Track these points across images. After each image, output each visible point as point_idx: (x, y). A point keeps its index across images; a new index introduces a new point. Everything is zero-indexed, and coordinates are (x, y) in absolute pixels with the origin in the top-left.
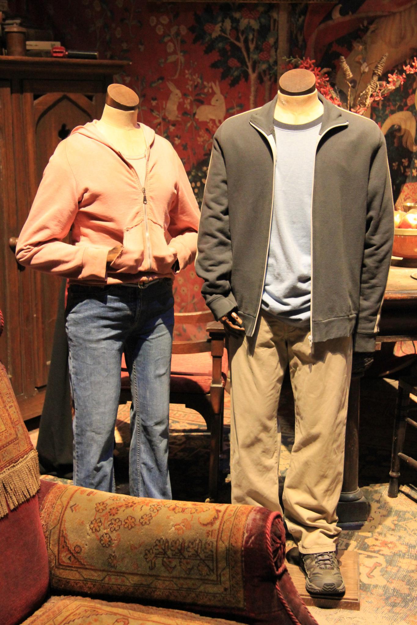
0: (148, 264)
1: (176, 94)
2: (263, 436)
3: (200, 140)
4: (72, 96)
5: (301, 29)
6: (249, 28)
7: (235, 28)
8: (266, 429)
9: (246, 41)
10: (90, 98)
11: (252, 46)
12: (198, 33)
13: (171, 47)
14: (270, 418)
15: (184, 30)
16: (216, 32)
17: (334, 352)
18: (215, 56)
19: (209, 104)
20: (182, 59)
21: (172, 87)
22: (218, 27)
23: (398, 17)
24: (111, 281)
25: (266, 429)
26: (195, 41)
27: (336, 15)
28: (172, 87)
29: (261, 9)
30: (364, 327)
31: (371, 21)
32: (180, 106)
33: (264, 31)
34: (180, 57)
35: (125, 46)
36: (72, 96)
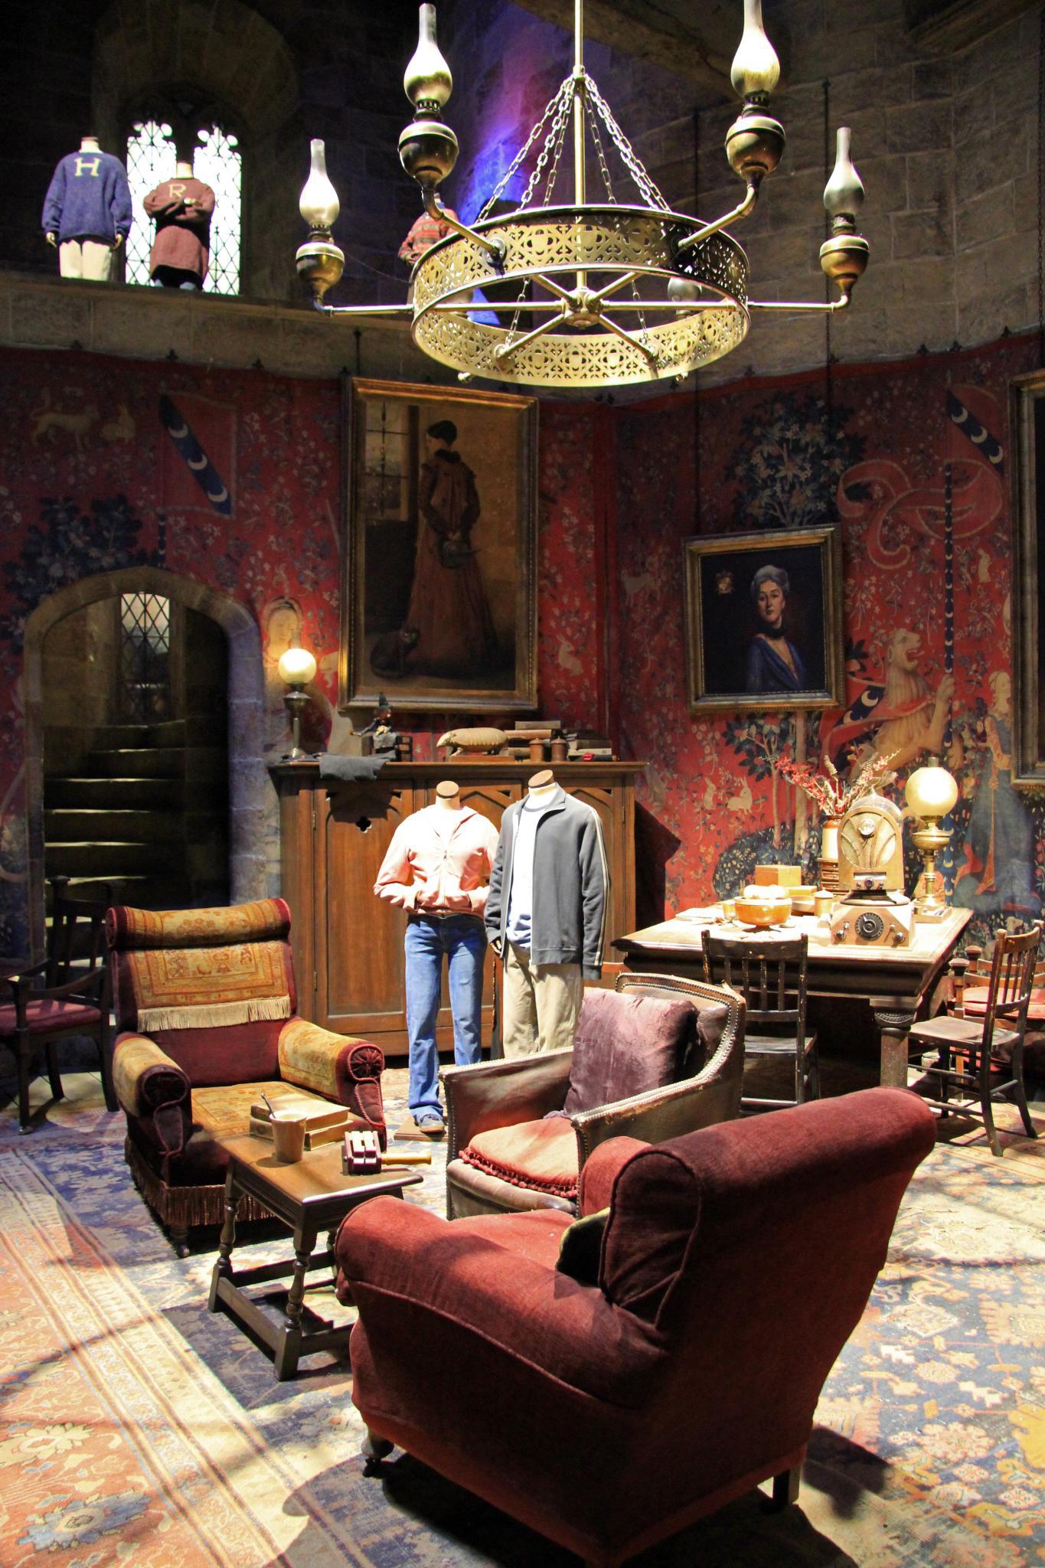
0: (439, 902)
1: (711, 787)
2: (517, 1035)
3: (731, 826)
4: (586, 790)
5: (816, 732)
6: (771, 732)
7: (760, 733)
8: (519, 1030)
9: (769, 743)
10: (609, 791)
11: (774, 747)
12: (729, 737)
13: (707, 750)
14: (523, 1023)
15: (718, 736)
16: (743, 735)
17: (552, 974)
18: (743, 756)
19: (738, 795)
20: (716, 759)
21: (708, 781)
22: (745, 732)
23: (905, 721)
24: (421, 911)
25: (519, 1030)
26: (727, 744)
27: (847, 720)
28: (708, 781)
29: (781, 716)
30: (586, 960)
31: (879, 724)
32: (715, 797)
33: (784, 735)
34: (715, 757)
35: (673, 749)
36: (586, 790)
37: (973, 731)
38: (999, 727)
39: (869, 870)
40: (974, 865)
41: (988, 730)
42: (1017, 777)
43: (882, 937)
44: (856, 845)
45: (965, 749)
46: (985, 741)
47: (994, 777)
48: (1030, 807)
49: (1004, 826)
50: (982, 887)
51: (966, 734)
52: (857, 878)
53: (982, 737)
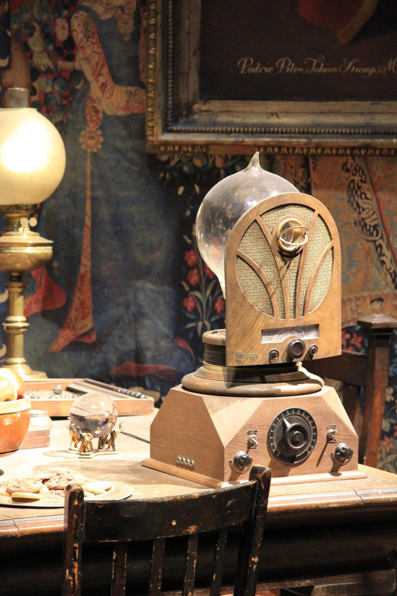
37: (49, 37)
38: (104, 33)
39: (291, 322)
40: (49, 295)
41: (79, 36)
42: (166, 129)
43: (314, 455)
44: (268, 273)
45: (34, 73)
46: (71, 58)
47: (92, 127)
48: (174, 184)
49: (116, 219)
50: (65, 337)
51: (36, 43)
52: (266, 340)
53: (67, 49)
